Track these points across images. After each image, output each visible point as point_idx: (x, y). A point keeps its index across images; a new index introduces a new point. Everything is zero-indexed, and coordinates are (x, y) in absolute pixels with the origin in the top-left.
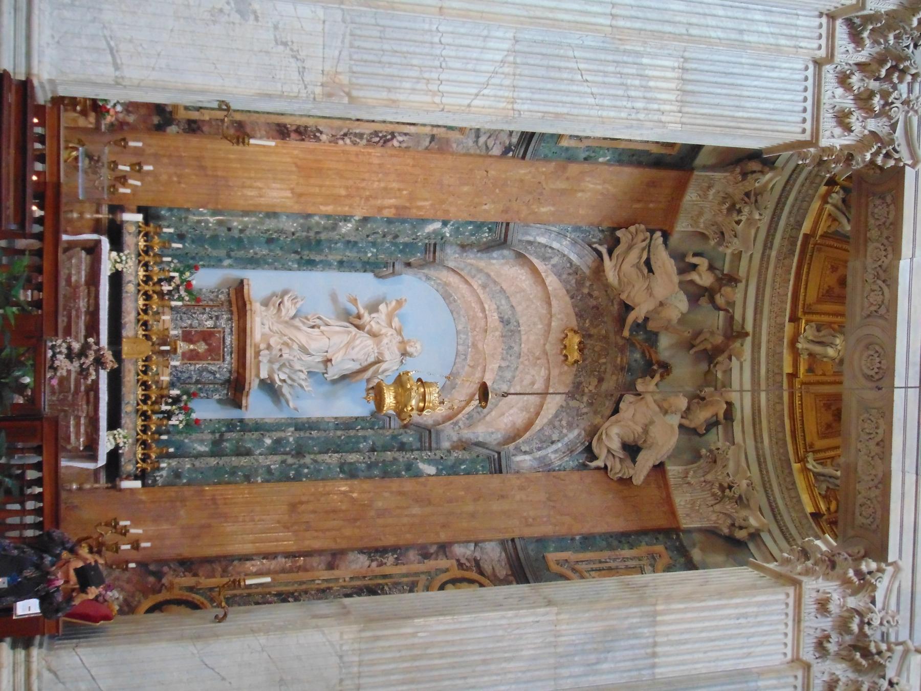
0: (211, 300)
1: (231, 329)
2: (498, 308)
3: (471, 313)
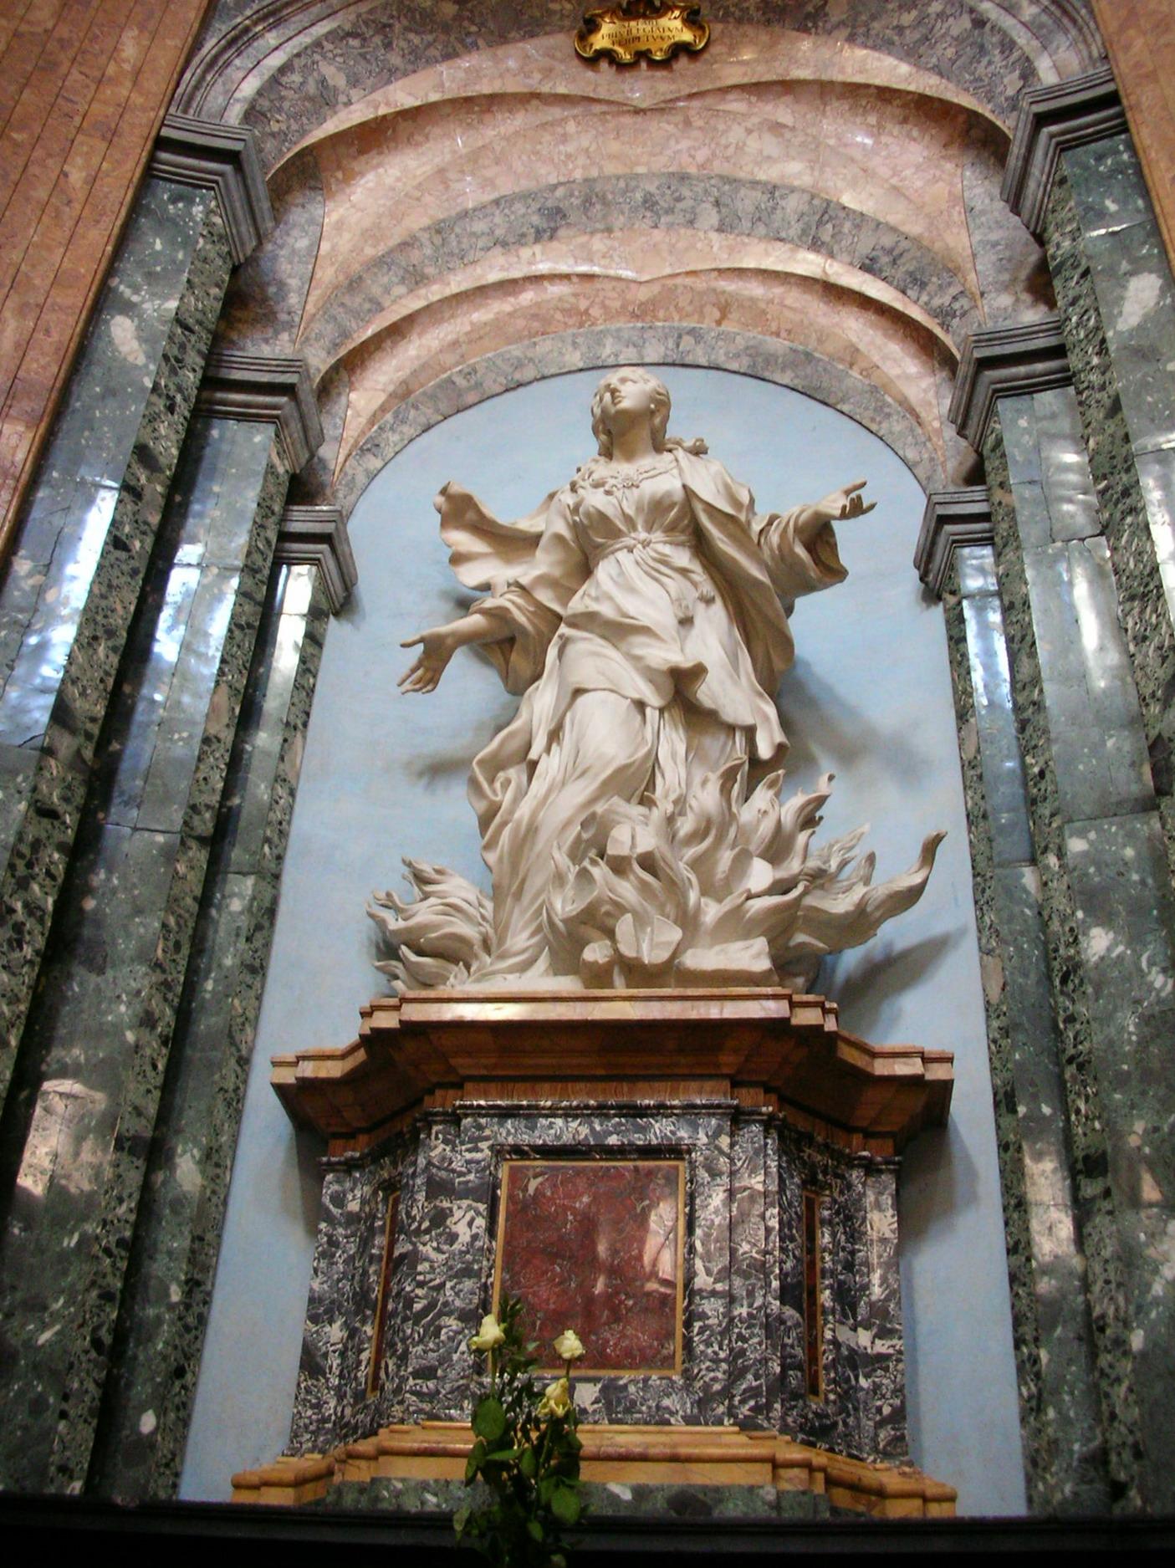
0: (365, 1243)
1: (504, 1114)
2: (505, 244)
3: (521, 323)
